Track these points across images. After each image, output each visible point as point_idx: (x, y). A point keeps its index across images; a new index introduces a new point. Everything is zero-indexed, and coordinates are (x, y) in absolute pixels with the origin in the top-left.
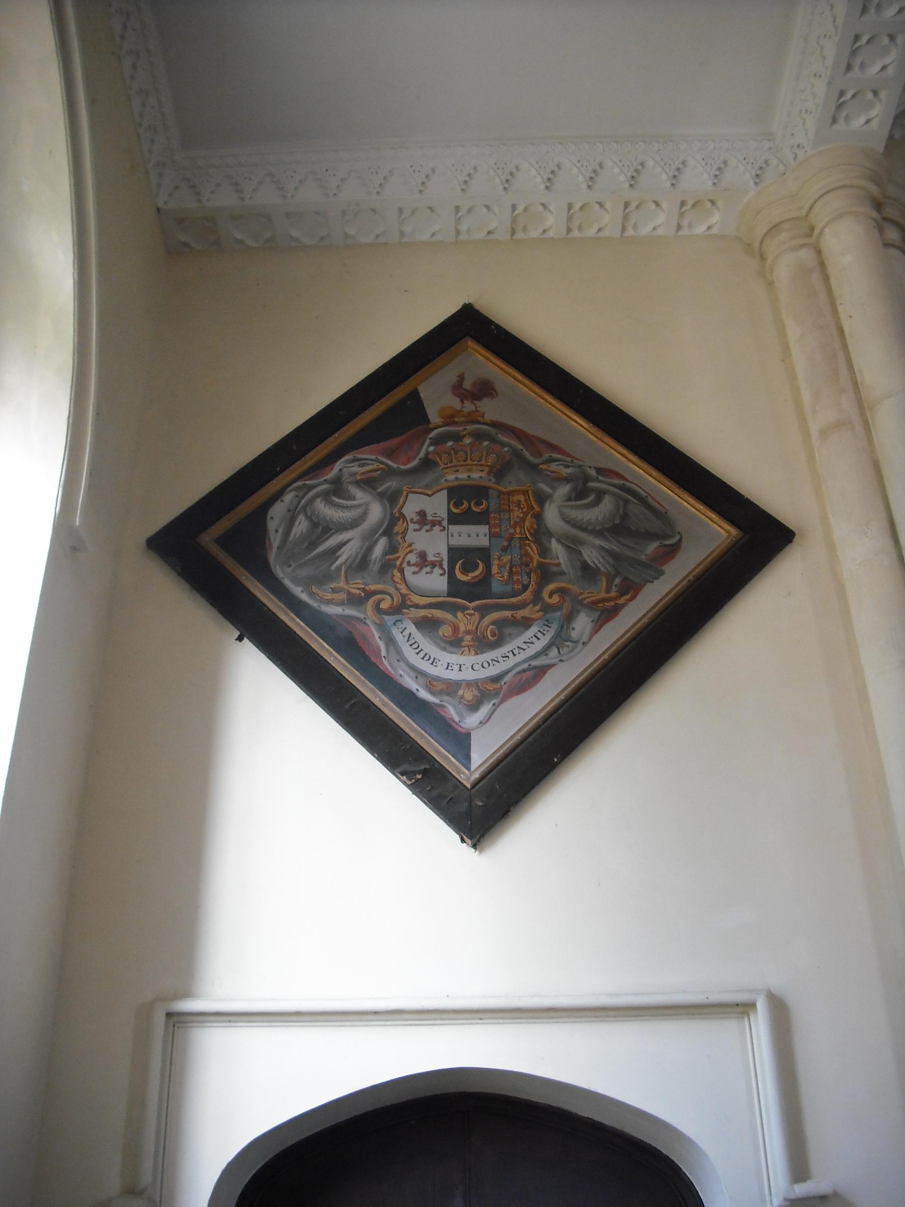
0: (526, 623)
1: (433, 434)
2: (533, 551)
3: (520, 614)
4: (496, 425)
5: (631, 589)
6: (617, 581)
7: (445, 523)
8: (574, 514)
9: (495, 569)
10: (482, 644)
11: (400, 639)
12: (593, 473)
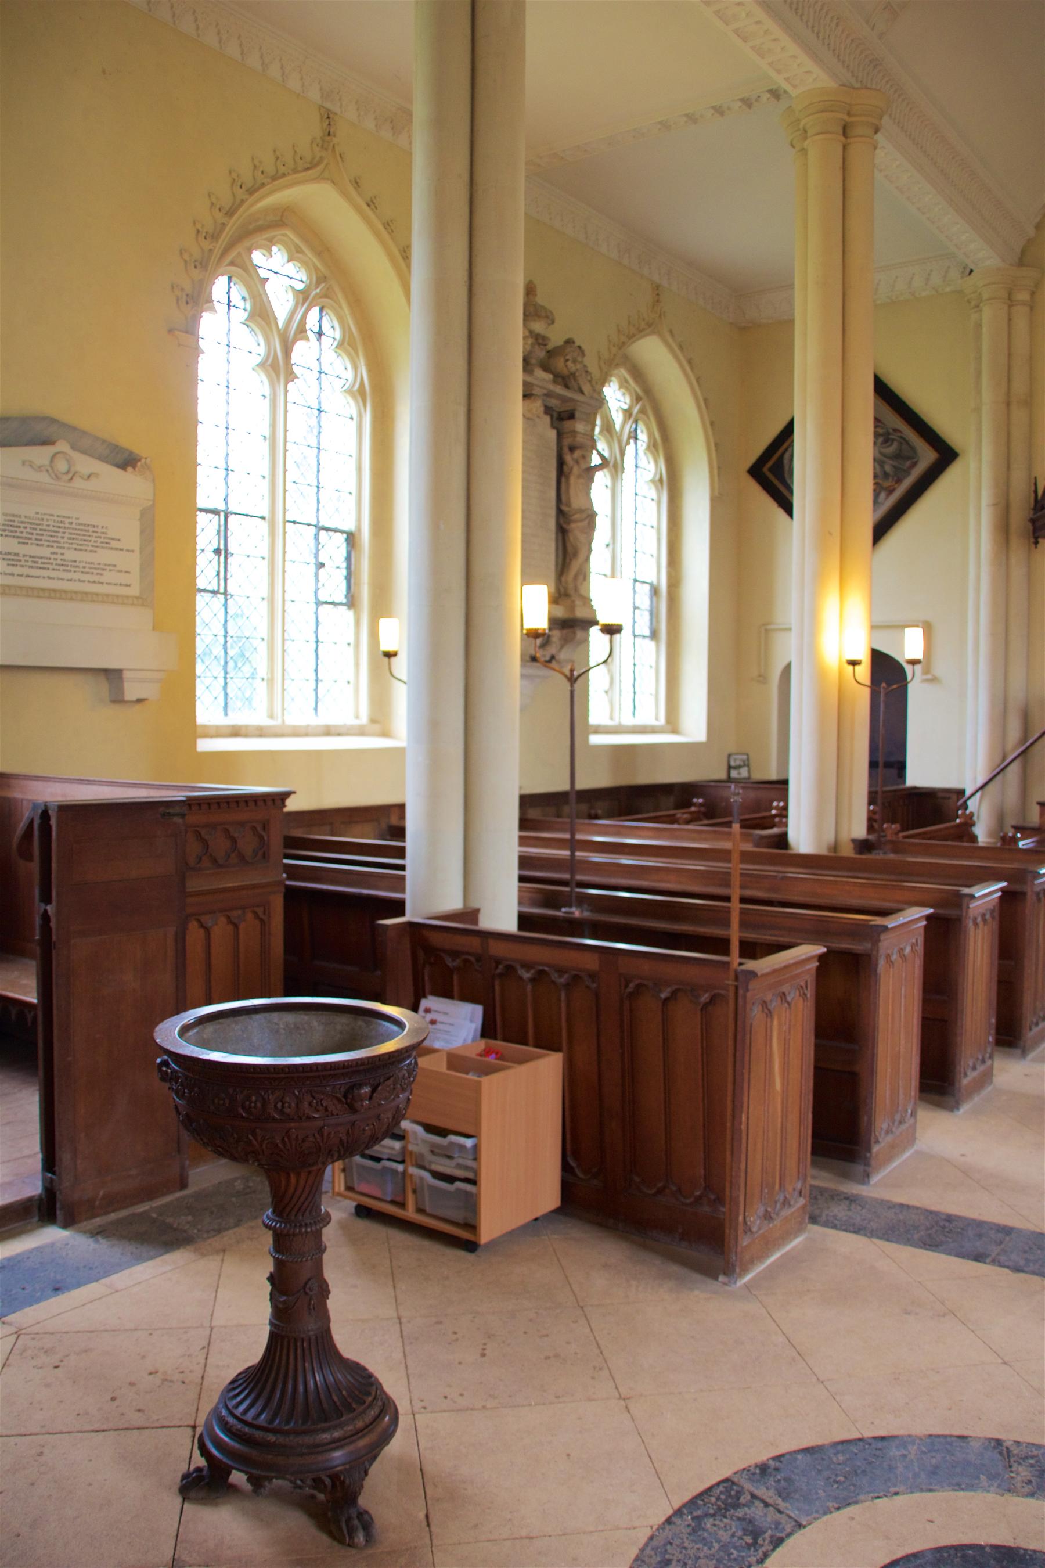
5: (899, 481)
8: (882, 450)
12: (891, 431)
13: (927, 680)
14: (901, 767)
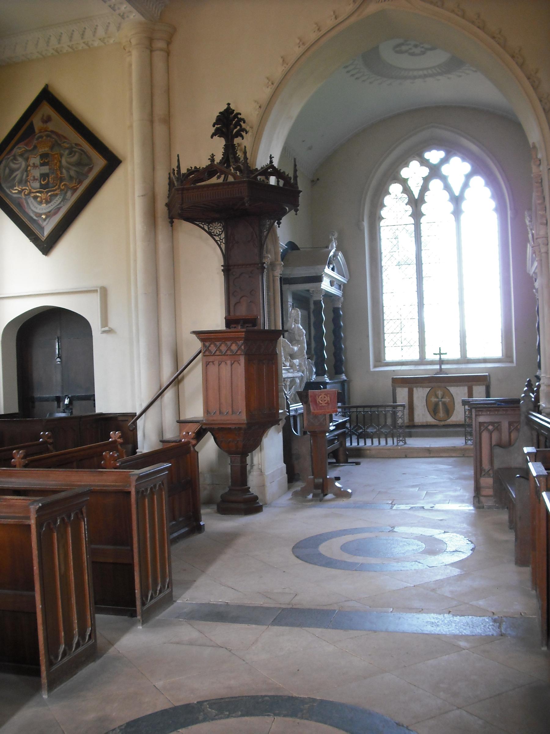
0: (56, 195)
1: (36, 136)
2: (59, 173)
3: (55, 192)
4: (52, 132)
5: (80, 182)
6: (78, 180)
7: (39, 166)
8: (69, 160)
9: (50, 180)
10: (47, 202)
11: (30, 202)
12: (74, 145)
13: (104, 332)
14: (91, 398)
